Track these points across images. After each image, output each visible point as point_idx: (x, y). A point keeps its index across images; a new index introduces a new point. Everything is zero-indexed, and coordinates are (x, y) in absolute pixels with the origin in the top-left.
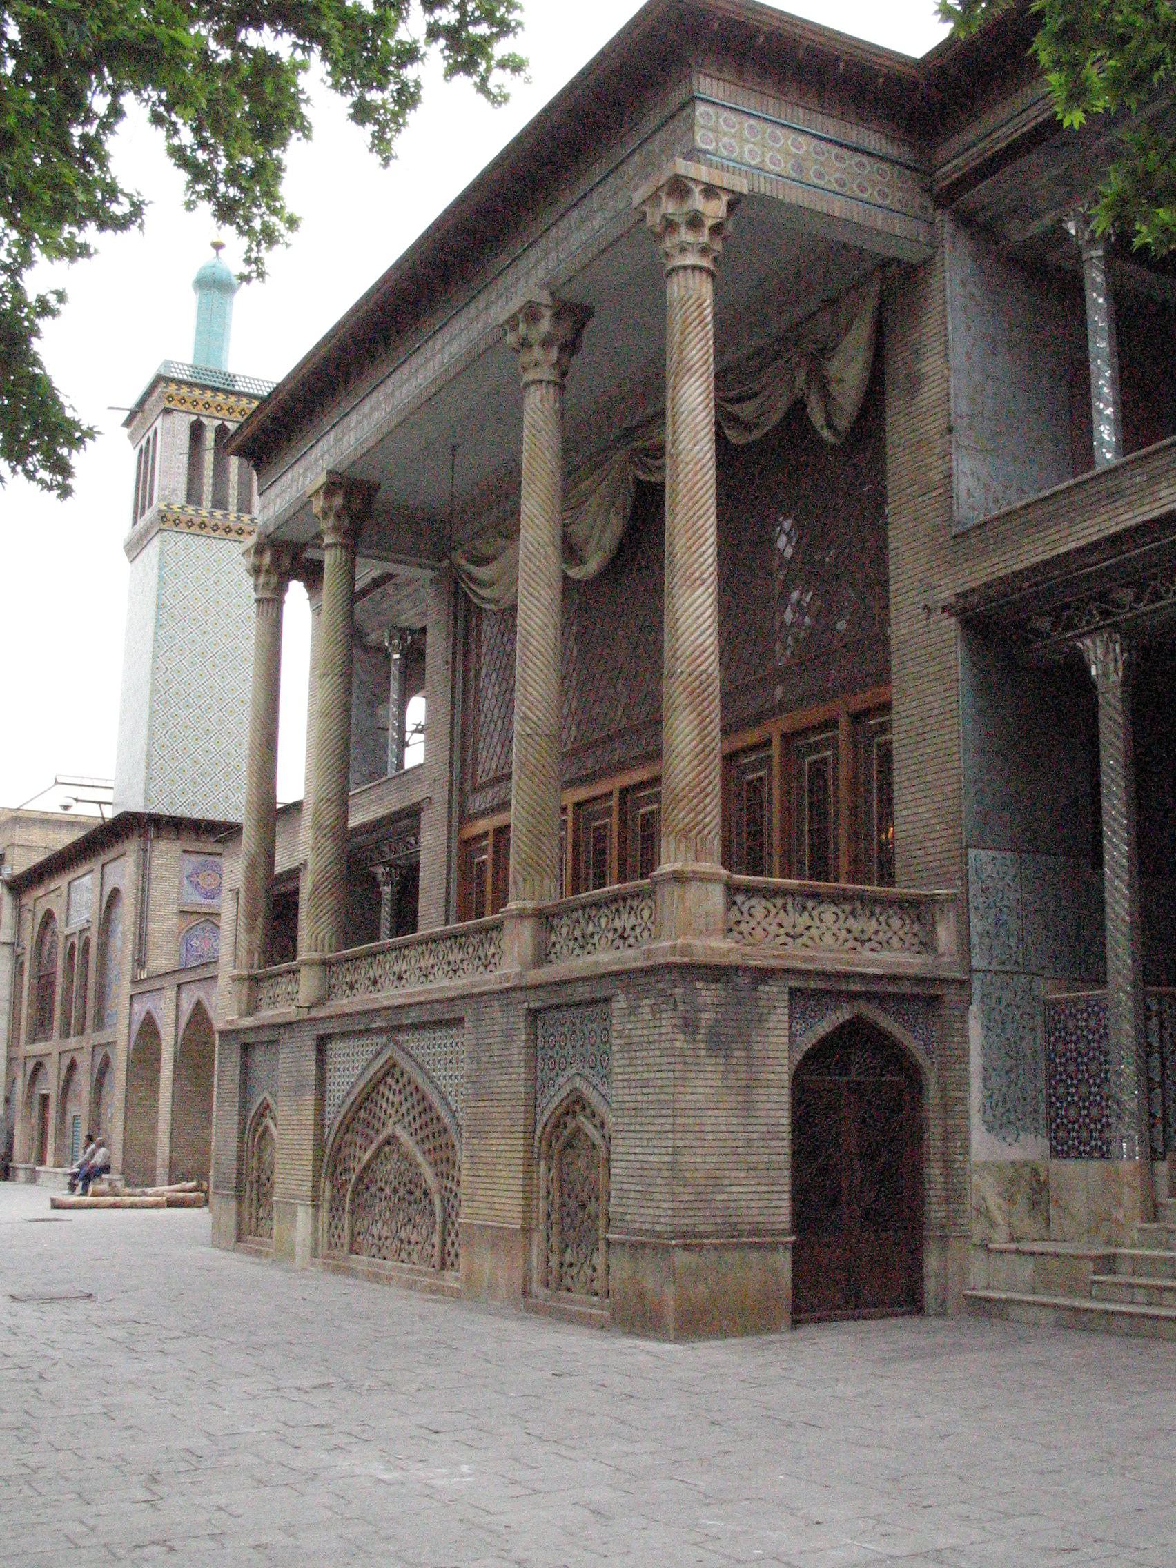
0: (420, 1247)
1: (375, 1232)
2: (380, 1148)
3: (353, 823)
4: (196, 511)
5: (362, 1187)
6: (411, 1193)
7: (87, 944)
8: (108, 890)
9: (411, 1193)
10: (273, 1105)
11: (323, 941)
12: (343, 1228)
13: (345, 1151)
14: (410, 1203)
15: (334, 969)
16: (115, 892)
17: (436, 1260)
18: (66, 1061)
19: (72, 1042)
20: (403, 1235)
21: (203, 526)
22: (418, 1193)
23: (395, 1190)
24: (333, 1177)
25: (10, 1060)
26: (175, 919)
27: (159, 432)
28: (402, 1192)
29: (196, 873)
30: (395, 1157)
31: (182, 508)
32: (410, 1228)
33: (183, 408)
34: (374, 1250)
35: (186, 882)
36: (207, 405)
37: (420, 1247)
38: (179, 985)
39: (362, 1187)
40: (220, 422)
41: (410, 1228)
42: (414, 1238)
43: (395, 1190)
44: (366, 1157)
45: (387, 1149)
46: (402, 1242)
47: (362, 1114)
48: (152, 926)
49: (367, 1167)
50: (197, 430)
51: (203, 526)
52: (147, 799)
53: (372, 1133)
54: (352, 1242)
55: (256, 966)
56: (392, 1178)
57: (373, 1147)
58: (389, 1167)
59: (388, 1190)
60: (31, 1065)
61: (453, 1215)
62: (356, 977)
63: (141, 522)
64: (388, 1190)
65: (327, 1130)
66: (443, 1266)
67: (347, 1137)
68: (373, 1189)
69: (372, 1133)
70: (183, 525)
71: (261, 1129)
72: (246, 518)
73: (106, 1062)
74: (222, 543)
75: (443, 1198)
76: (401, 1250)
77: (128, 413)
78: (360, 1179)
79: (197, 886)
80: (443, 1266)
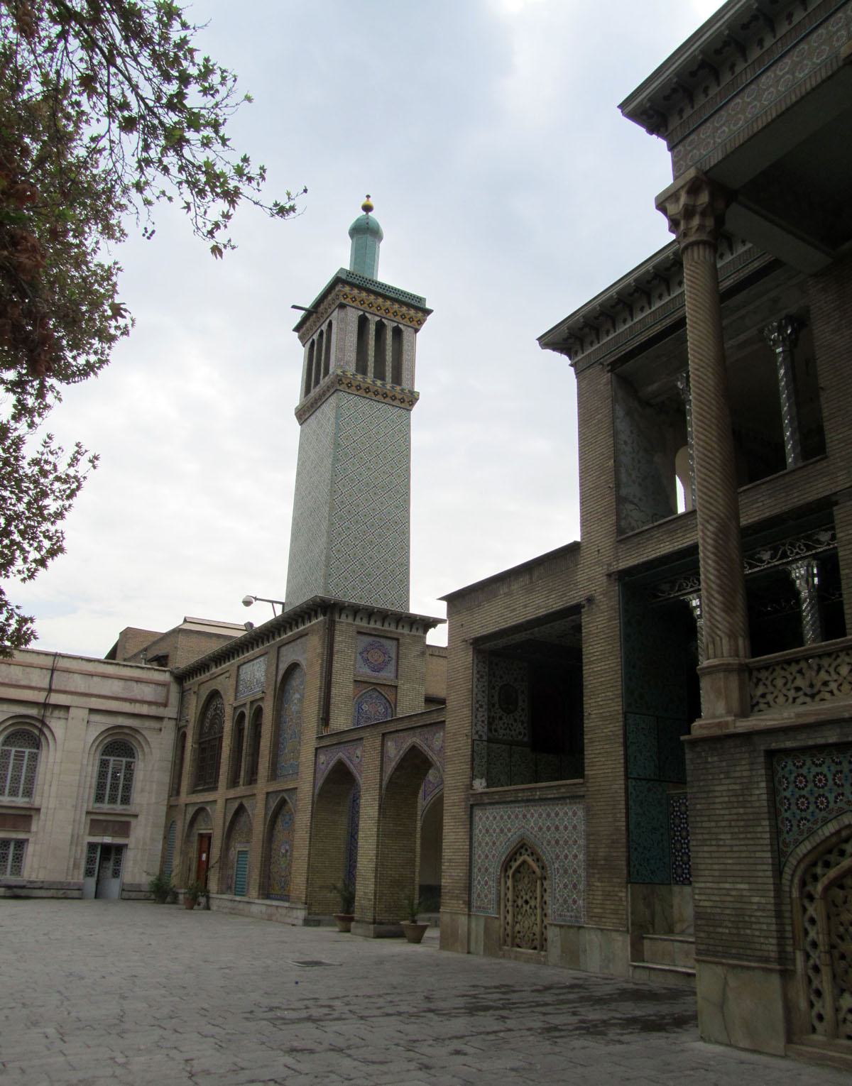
3: (744, 522)
4: (364, 378)
7: (259, 712)
8: (283, 667)
16: (294, 667)
19: (241, 790)
21: (367, 390)
25: (171, 808)
26: (352, 686)
27: (334, 323)
29: (366, 650)
31: (353, 375)
33: (353, 305)
35: (359, 657)
36: (371, 306)
38: (384, 735)
40: (379, 319)
48: (334, 691)
50: (363, 322)
51: (367, 390)
52: (326, 589)
60: (191, 811)
63: (315, 392)
70: (354, 388)
72: (398, 388)
74: (381, 405)
77: (302, 313)
79: (366, 661)
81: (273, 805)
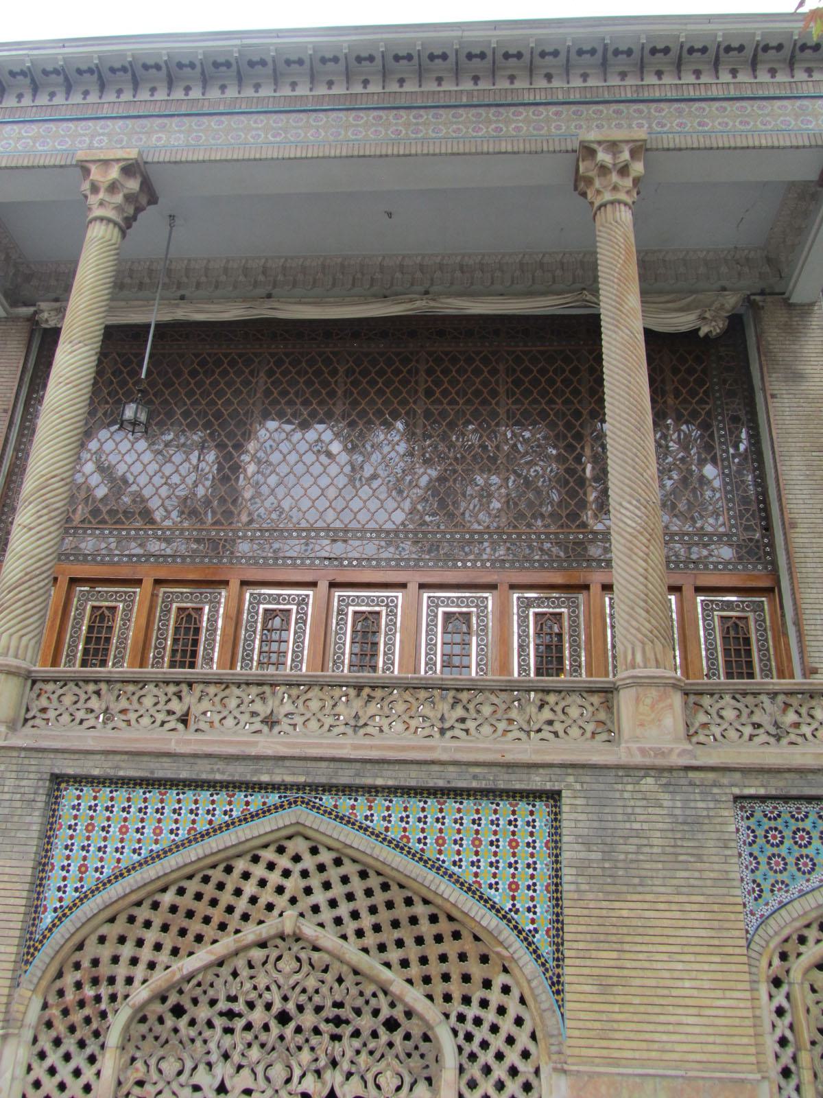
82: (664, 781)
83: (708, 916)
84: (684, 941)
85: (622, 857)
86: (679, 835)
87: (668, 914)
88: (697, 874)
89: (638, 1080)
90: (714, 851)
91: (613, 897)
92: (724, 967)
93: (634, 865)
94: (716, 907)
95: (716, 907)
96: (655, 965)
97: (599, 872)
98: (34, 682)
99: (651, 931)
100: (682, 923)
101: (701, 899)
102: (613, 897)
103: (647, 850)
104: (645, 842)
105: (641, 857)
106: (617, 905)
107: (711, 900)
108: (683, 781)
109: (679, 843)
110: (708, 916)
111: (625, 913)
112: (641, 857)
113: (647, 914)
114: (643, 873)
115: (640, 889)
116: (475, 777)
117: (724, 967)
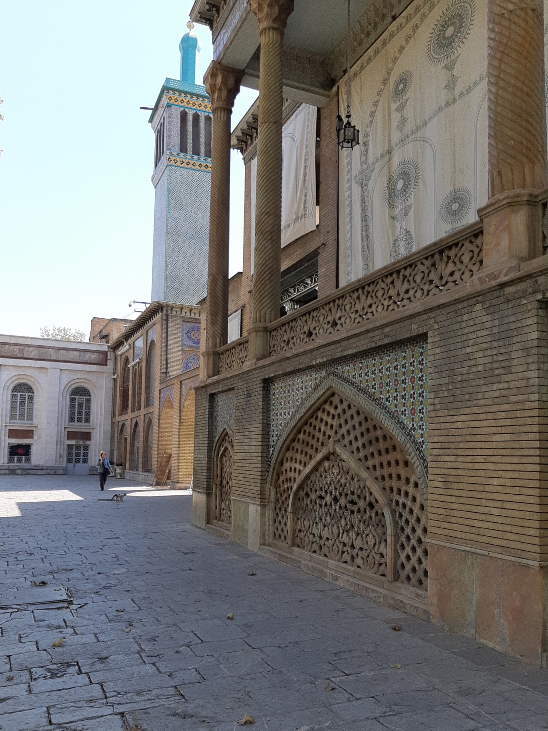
0: (365, 553)
1: (315, 531)
2: (320, 463)
5: (302, 494)
6: (353, 503)
9: (353, 503)
10: (230, 433)
11: (265, 314)
12: (285, 524)
13: (287, 465)
14: (352, 512)
15: (273, 333)
17: (389, 571)
18: (134, 422)
19: (136, 413)
20: (345, 538)
22: (361, 504)
23: (336, 500)
24: (277, 487)
25: (113, 424)
28: (343, 501)
30: (335, 471)
32: (352, 534)
34: (315, 547)
37: (365, 553)
39: (302, 494)
41: (352, 534)
42: (358, 543)
43: (336, 500)
44: (308, 470)
45: (326, 464)
46: (344, 544)
47: (301, 436)
49: (308, 477)
53: (310, 451)
54: (294, 537)
55: (218, 345)
56: (332, 488)
57: (313, 463)
58: (329, 480)
59: (328, 499)
60: (120, 424)
61: (408, 531)
62: (292, 334)
64: (328, 499)
65: (271, 449)
66: (396, 577)
67: (289, 455)
68: (313, 496)
69: (310, 451)
71: (222, 449)
73: (150, 421)
75: (393, 512)
76: (343, 552)
78: (301, 487)
80: (396, 577)
81: (147, 421)
82: (487, 304)
83: (512, 422)
84: (487, 445)
85: (459, 379)
86: (495, 352)
87: (485, 423)
88: (505, 385)
89: (463, 553)
90: (522, 361)
91: (453, 413)
92: (521, 467)
93: (465, 384)
94: (518, 414)
95: (518, 414)
96: (477, 466)
97: (446, 394)
98: (271, 332)
99: (474, 438)
100: (494, 430)
101: (507, 407)
102: (453, 413)
103: (474, 369)
104: (473, 362)
105: (471, 376)
106: (456, 418)
107: (516, 407)
108: (500, 300)
109: (495, 358)
110: (512, 422)
111: (459, 425)
112: (471, 376)
113: (473, 424)
114: (471, 390)
115: (469, 403)
116: (387, 336)
117: (521, 467)
